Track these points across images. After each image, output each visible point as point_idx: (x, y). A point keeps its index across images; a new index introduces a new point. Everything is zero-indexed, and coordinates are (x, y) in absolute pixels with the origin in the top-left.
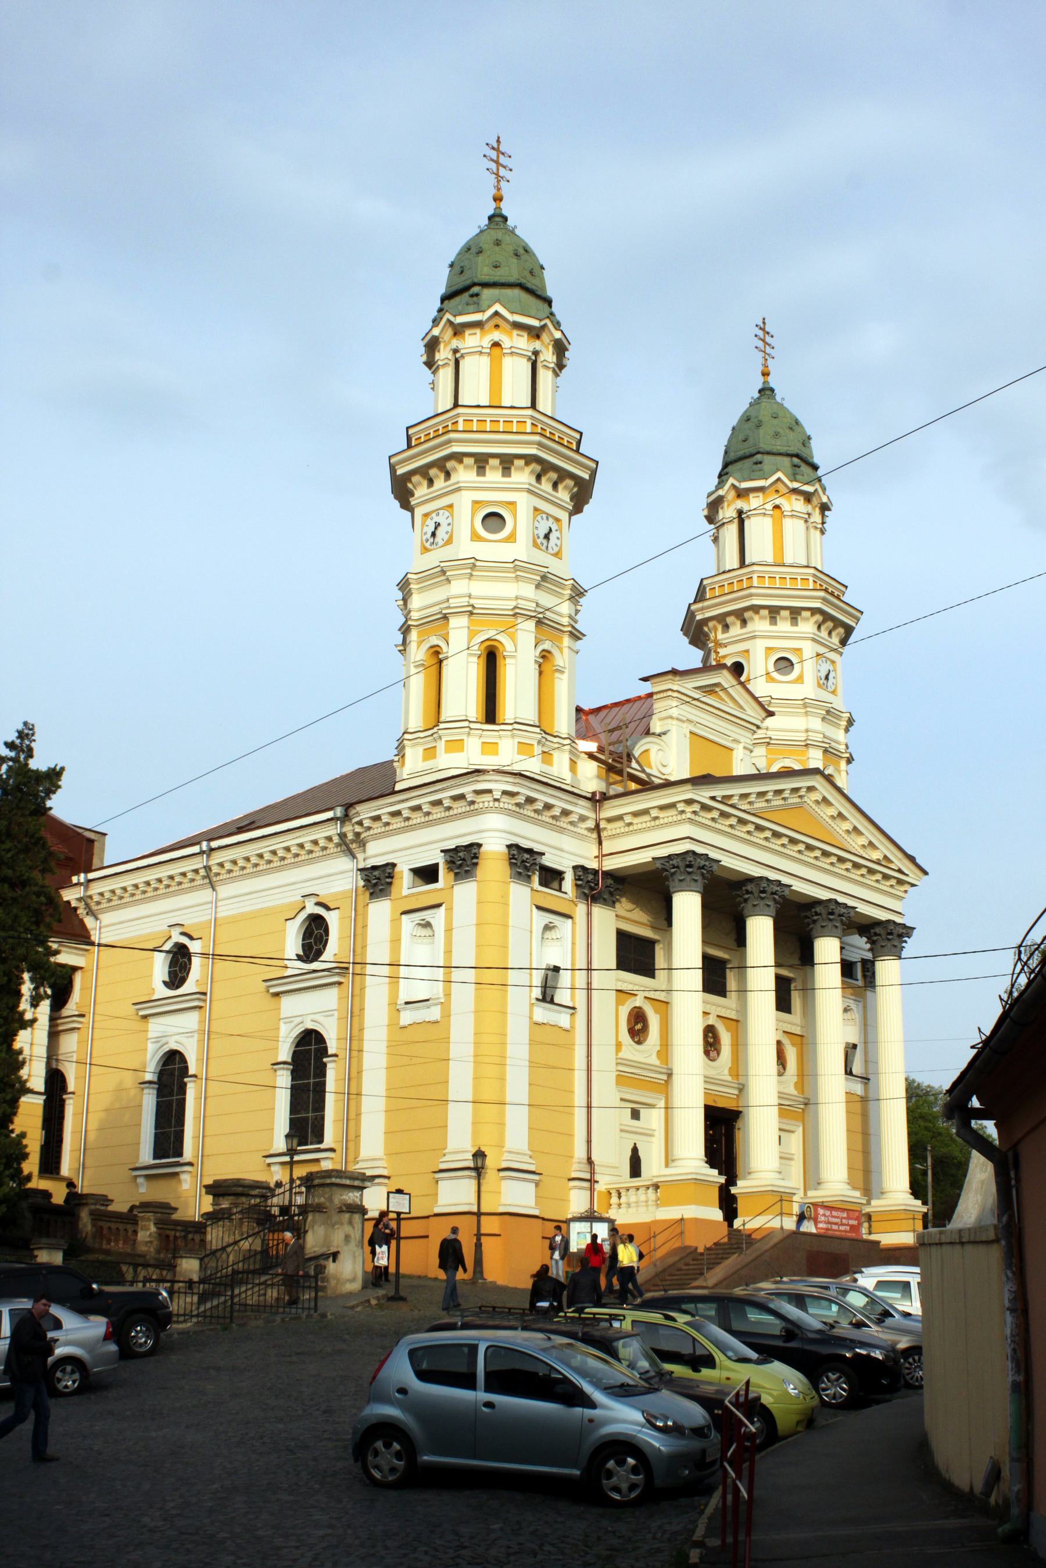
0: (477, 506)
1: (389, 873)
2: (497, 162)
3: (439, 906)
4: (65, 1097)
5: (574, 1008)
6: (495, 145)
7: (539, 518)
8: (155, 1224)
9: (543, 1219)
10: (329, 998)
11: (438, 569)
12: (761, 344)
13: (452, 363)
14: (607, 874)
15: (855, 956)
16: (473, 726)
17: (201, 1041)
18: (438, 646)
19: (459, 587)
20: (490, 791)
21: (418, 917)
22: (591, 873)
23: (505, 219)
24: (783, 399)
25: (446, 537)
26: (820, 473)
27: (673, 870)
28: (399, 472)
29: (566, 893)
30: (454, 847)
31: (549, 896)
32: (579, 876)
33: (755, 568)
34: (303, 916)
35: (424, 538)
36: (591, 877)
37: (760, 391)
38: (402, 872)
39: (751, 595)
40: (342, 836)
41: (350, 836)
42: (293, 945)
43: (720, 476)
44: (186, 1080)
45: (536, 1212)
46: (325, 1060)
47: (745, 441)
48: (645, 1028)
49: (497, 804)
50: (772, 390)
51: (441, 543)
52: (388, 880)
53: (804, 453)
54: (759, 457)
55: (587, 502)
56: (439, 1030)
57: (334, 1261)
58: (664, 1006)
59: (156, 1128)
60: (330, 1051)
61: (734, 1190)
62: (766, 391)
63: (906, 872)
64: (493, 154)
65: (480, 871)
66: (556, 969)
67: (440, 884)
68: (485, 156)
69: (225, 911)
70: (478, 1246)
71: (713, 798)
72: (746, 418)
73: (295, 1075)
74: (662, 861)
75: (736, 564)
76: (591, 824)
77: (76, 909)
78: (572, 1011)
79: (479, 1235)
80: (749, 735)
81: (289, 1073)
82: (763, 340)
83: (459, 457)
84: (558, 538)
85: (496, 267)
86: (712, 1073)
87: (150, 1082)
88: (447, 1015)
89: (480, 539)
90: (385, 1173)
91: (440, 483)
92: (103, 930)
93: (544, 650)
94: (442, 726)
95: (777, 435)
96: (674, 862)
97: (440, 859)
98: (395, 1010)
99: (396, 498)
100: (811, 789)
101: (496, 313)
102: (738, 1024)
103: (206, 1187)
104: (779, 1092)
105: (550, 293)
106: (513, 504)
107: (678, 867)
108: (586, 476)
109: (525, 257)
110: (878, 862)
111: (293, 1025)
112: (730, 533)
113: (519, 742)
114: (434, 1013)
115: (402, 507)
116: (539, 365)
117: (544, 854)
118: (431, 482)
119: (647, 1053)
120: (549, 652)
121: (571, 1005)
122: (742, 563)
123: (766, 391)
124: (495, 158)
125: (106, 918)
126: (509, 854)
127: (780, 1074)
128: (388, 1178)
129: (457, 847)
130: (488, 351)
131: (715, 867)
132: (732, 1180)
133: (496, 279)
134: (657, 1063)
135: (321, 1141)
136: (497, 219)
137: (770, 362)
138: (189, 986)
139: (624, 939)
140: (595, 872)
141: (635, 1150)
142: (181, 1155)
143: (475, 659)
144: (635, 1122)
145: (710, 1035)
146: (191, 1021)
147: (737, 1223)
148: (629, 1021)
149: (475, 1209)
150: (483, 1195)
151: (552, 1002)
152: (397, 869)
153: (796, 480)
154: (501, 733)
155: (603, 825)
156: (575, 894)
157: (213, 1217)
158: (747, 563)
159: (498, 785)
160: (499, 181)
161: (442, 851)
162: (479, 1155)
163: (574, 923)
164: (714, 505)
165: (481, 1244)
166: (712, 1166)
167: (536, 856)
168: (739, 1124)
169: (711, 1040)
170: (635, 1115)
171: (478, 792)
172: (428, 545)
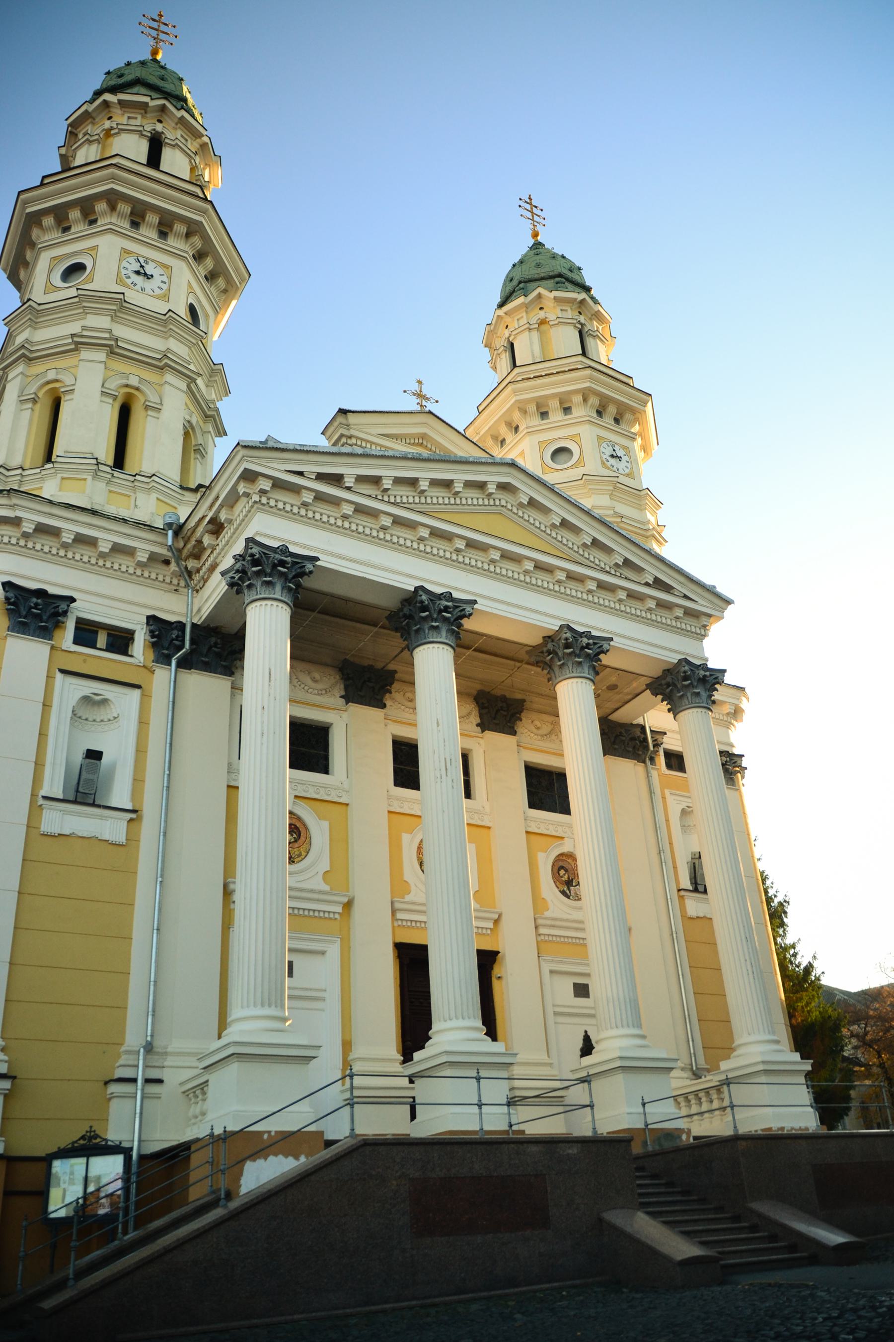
5: (134, 811)
12: (529, 215)
22: (176, 628)
26: (592, 292)
29: (132, 656)
36: (175, 633)
53: (574, 276)
54: (521, 285)
62: (537, 246)
66: (94, 755)
71: (300, 474)
74: (231, 574)
100: (504, 487)
113: (63, 478)
117: (72, 600)
120: (137, 389)
121: (129, 806)
123: (537, 246)
140: (181, 626)
143: (30, 405)
154: (44, 473)
156: (151, 655)
163: (143, 695)
167: (59, 603)
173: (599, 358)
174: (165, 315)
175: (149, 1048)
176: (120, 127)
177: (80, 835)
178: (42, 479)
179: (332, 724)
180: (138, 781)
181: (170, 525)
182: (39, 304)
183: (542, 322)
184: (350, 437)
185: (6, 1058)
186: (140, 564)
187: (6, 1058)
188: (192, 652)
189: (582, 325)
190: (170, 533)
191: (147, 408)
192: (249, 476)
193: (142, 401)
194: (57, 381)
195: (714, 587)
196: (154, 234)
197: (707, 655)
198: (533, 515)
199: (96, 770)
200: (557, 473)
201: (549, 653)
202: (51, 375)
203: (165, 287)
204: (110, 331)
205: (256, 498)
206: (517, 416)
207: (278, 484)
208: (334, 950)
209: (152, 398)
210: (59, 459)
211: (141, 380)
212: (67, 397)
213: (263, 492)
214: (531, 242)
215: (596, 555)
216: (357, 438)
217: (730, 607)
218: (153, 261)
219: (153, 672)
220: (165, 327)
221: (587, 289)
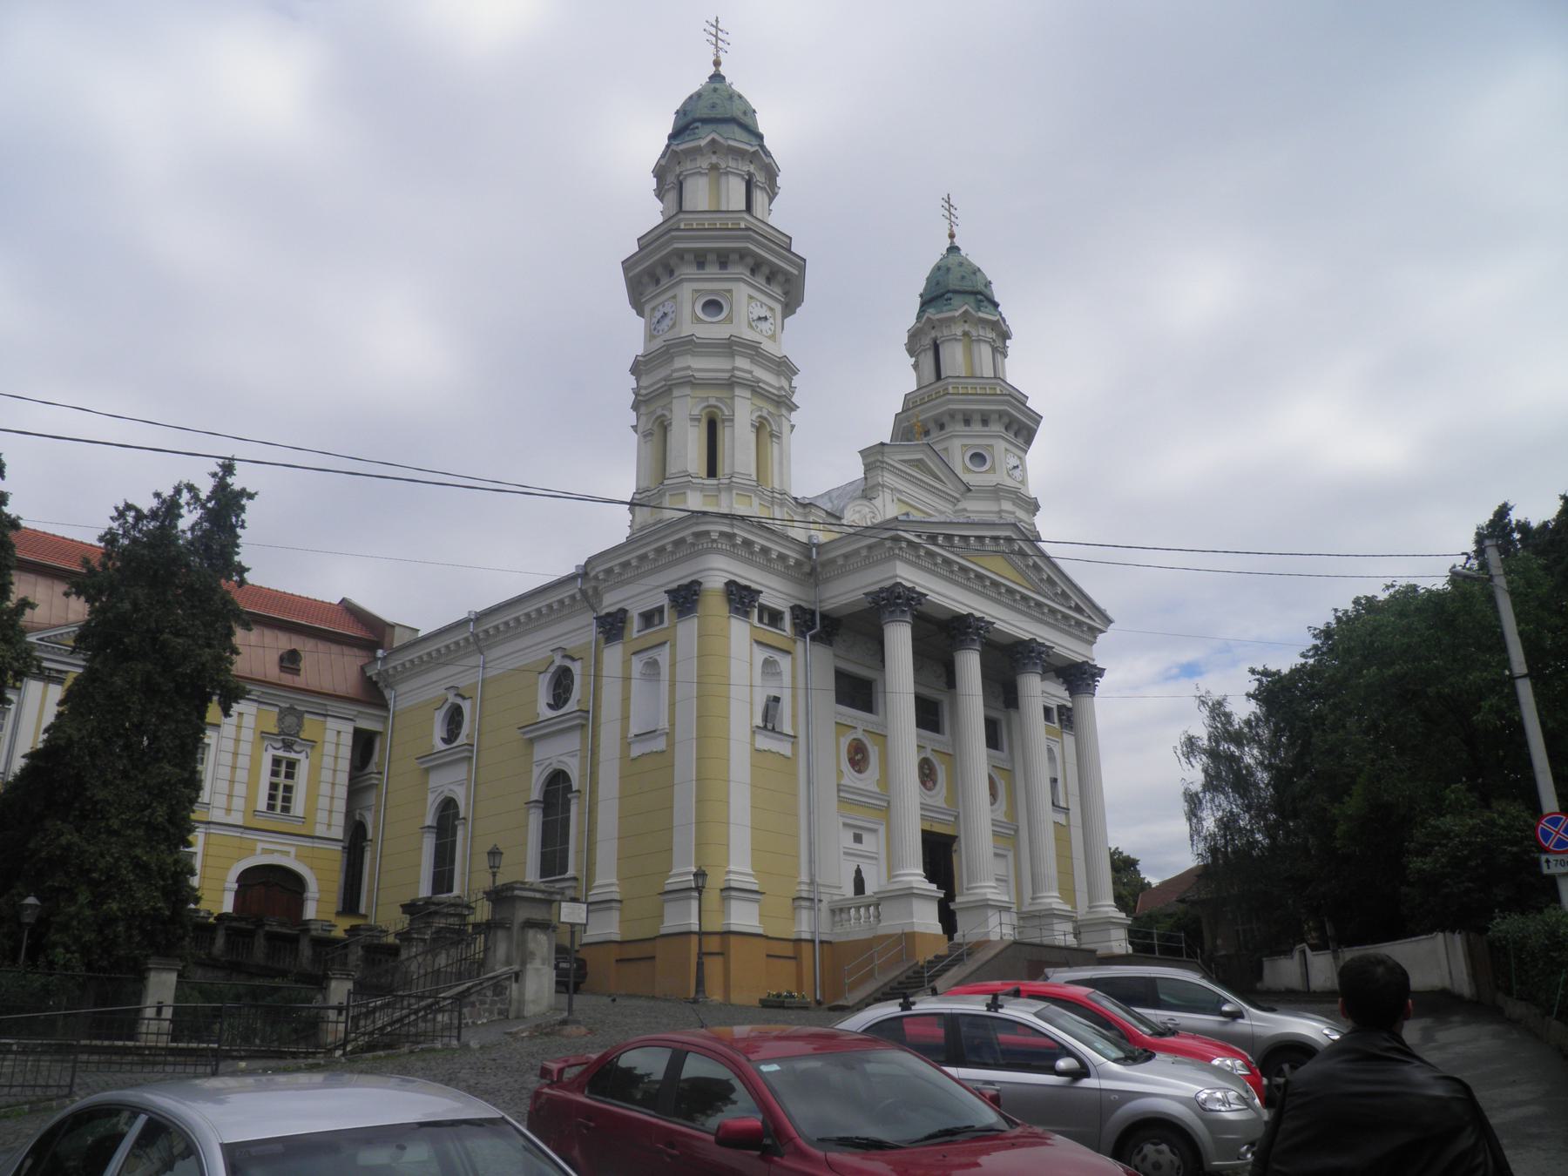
0: (696, 295)
1: (621, 619)
2: (716, 36)
3: (663, 643)
4: (364, 844)
5: (795, 737)
6: (715, 24)
7: (753, 304)
8: (362, 947)
9: (767, 937)
10: (573, 742)
11: (665, 348)
12: (947, 214)
13: (677, 187)
14: (824, 616)
15: (1053, 704)
16: (694, 481)
17: (468, 789)
18: (664, 415)
19: (679, 363)
20: (707, 533)
21: (645, 656)
23: (724, 78)
24: (967, 255)
25: (670, 323)
26: (1000, 309)
27: (883, 603)
28: (630, 275)
29: (784, 631)
30: (674, 585)
31: (770, 634)
32: (797, 615)
33: (950, 380)
34: (552, 669)
35: (653, 327)
36: (808, 617)
37: (948, 250)
38: (633, 617)
39: (949, 400)
40: (583, 592)
41: (590, 592)
42: (543, 696)
43: (917, 319)
44: (456, 823)
45: (760, 931)
46: (569, 796)
47: (938, 283)
48: (865, 759)
49: (715, 546)
50: (958, 249)
51: (666, 328)
52: (620, 625)
53: (986, 291)
54: (949, 295)
55: (799, 305)
56: (665, 758)
57: (517, 981)
58: (882, 738)
59: (435, 868)
60: (575, 788)
61: (952, 906)
62: (953, 249)
63: (1094, 618)
64: (713, 31)
65: (700, 608)
66: (777, 699)
67: (666, 624)
68: (705, 30)
69: (491, 673)
70: (700, 965)
72: (938, 268)
73: (546, 813)
75: (932, 378)
76: (807, 569)
77: (376, 683)
78: (792, 740)
79: (701, 955)
80: (951, 507)
81: (540, 811)
82: (949, 211)
83: (680, 255)
84: (772, 324)
85: (713, 107)
86: (929, 801)
87: (429, 827)
88: (671, 744)
89: (700, 321)
90: (617, 897)
91: (665, 282)
92: (398, 699)
93: (760, 417)
94: (666, 482)
95: (963, 278)
96: (884, 595)
97: (664, 600)
98: (626, 744)
99: (633, 307)
100: (1009, 540)
101: (713, 140)
102: (953, 757)
103: (402, 906)
104: (993, 820)
105: (761, 130)
106: (730, 291)
107: (887, 599)
108: (796, 272)
109: (738, 102)
110: (1070, 608)
111: (543, 766)
112: (928, 360)
113: (737, 494)
114: (660, 744)
115: (638, 314)
116: (753, 186)
117: (761, 592)
118: (657, 282)
119: (868, 781)
120: (765, 419)
122: (938, 377)
123: (953, 249)
124: (714, 33)
125: (402, 688)
126: (727, 590)
127: (992, 804)
128: (620, 901)
129: (679, 586)
130: (707, 171)
131: (923, 600)
132: (950, 896)
133: (713, 116)
134: (877, 790)
135: (566, 871)
136: (717, 77)
137: (955, 228)
138: (462, 739)
139: (840, 675)
140: (813, 613)
141: (858, 872)
142: (450, 890)
143: (696, 423)
144: (858, 846)
145: (926, 767)
146: (461, 772)
147: (958, 937)
148: (849, 752)
149: (695, 928)
150: (702, 913)
151: (773, 729)
152: (629, 614)
153: (980, 310)
155: (819, 569)
157: (405, 936)
158: (942, 377)
159: (716, 528)
160: (717, 51)
161: (666, 592)
162: (700, 875)
163: (792, 658)
164: (914, 337)
165: (703, 964)
166: (931, 881)
168: (955, 847)
169: (928, 772)
170: (858, 839)
171: (697, 535)
172: (655, 333)
173: (1005, 375)
174: (780, 358)
175: (812, 883)
176: (728, 169)
177: (773, 750)
178: (719, 490)
179: (875, 680)
180: (794, 716)
181: (814, 544)
182: (697, 338)
183: (966, 334)
184: (882, 462)
185: (756, 881)
186: (788, 567)
187: (756, 881)
188: (820, 632)
189: (994, 341)
190: (814, 549)
191: (772, 435)
192: (896, 539)
193: (769, 429)
194: (715, 407)
195: (1105, 611)
196: (764, 283)
197: (1094, 656)
198: (1017, 559)
199: (776, 708)
200: (975, 475)
201: (1018, 653)
202: (712, 402)
203: (773, 328)
204: (751, 372)
205: (897, 551)
206: (946, 419)
207: (910, 543)
208: (882, 829)
209: (774, 428)
210: (734, 479)
211: (769, 413)
212: (726, 424)
213: (901, 548)
214: (947, 243)
215: (1045, 588)
216: (887, 463)
217: (1112, 625)
218: (766, 305)
219: (795, 642)
220: (779, 367)
221: (996, 305)
